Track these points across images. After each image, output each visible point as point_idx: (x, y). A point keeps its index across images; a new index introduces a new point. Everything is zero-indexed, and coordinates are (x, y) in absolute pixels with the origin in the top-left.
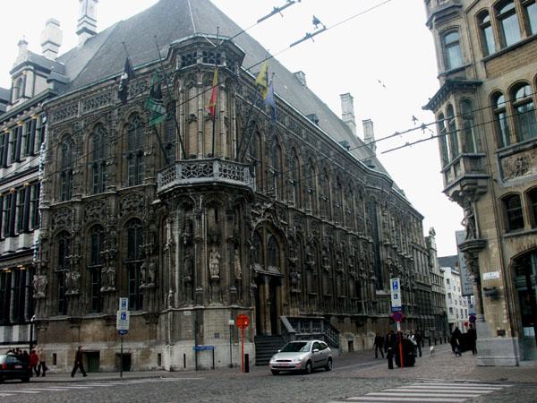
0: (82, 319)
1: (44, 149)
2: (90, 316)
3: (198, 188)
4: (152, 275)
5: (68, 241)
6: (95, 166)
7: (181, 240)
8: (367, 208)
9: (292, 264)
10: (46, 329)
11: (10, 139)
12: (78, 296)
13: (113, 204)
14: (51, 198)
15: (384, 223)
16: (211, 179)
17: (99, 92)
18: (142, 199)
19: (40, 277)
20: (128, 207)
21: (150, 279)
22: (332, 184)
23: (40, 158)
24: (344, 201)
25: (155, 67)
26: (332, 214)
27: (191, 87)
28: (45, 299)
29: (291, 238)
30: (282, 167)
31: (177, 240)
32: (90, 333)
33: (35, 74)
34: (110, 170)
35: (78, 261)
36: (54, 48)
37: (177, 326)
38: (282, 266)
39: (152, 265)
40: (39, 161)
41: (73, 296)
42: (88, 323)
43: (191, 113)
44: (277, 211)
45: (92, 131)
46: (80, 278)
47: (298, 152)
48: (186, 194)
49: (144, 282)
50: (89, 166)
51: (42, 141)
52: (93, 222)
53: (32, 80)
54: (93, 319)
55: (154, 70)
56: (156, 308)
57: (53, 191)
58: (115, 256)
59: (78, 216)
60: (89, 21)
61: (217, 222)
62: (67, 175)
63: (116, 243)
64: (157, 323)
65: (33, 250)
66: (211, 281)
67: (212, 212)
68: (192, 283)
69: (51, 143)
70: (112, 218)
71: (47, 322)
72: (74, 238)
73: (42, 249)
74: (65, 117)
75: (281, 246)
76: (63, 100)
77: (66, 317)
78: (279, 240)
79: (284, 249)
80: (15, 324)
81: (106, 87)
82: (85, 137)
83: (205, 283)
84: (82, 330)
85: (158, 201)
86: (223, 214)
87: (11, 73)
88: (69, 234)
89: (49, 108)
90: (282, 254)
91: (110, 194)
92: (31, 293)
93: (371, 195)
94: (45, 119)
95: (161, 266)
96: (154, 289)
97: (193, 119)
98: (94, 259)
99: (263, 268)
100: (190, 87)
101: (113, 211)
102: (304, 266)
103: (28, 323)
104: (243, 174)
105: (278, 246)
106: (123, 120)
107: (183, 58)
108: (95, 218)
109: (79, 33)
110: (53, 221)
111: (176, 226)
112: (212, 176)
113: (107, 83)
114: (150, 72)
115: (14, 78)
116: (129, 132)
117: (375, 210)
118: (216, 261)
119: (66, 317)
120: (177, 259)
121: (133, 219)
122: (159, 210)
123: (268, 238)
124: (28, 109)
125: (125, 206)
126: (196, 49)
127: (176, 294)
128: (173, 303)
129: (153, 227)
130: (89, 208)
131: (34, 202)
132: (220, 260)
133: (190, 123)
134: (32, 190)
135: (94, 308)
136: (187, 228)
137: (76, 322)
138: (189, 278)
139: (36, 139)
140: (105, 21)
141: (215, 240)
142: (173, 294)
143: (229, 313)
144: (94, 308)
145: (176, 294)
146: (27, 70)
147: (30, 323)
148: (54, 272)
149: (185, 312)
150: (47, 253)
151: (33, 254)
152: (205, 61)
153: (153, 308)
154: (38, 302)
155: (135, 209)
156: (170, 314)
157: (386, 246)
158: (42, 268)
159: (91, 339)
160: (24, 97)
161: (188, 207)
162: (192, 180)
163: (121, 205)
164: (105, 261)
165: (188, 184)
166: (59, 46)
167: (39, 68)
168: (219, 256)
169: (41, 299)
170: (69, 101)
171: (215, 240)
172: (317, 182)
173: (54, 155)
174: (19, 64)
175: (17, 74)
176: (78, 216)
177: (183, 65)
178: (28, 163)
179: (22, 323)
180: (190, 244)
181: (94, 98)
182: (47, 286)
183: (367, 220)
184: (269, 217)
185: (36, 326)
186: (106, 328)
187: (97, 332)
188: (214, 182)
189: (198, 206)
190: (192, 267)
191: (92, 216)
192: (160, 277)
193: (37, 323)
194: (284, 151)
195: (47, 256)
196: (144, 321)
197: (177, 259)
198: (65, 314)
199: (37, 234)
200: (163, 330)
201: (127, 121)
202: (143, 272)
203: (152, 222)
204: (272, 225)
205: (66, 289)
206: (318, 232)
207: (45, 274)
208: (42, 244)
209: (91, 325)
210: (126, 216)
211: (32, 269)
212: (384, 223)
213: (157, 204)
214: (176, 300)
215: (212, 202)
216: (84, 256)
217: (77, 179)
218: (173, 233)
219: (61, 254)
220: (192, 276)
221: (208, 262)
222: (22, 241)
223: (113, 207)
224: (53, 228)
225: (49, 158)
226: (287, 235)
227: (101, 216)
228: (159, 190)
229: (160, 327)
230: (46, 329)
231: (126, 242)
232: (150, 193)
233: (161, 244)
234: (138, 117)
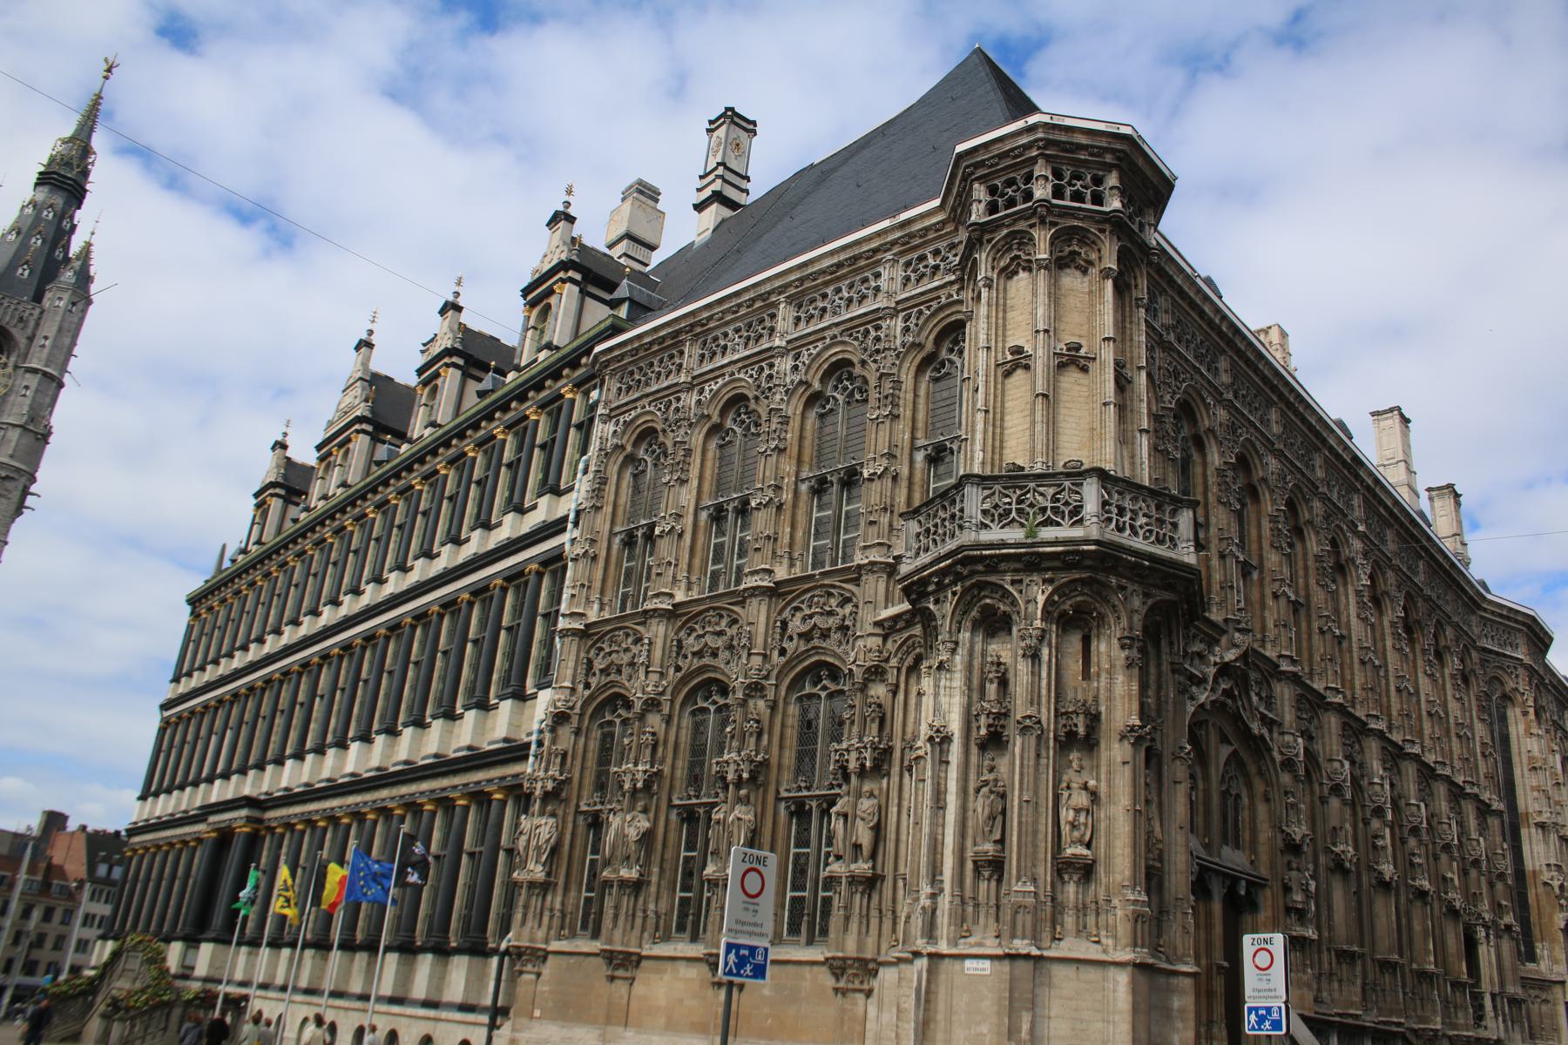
1: (585, 472)
3: (1031, 562)
4: (864, 836)
5: (625, 722)
6: (718, 515)
7: (969, 720)
8: (1481, 709)
9: (1293, 848)
11: (508, 455)
12: (637, 886)
13: (763, 619)
14: (588, 601)
15: (1531, 759)
16: (1078, 533)
18: (848, 609)
19: (537, 821)
20: (804, 628)
21: (857, 847)
22: (1393, 624)
23: (574, 495)
24: (1424, 683)
26: (1394, 713)
27: (1016, 273)
28: (545, 887)
29: (1288, 764)
30: (1261, 548)
31: (955, 726)
32: (662, 1002)
33: (584, 293)
34: (762, 521)
35: (648, 785)
36: (640, 252)
37: (941, 1007)
38: (1263, 850)
39: (866, 804)
40: (567, 505)
41: (623, 883)
42: (658, 972)
43: (1011, 343)
44: (1253, 675)
45: (716, 418)
46: (647, 838)
47: (1305, 515)
48: (993, 579)
49: (838, 858)
50: (704, 515)
51: (584, 451)
53: (574, 306)
56: (871, 941)
57: (597, 585)
58: (758, 774)
59: (657, 654)
60: (729, 176)
61: (1086, 674)
62: (639, 540)
63: (760, 735)
64: (869, 994)
65: (528, 745)
66: (1063, 867)
67: (1074, 643)
68: (996, 866)
70: (757, 661)
71: (544, 956)
72: (641, 717)
73: (554, 741)
74: (647, 384)
75: (1259, 787)
77: (596, 946)
78: (1252, 769)
79: (1267, 800)
80: (459, 951)
82: (697, 438)
83: (1045, 872)
84: (638, 988)
85: (906, 606)
86: (1108, 649)
87: (526, 292)
88: (628, 705)
89: (607, 364)
90: (1262, 809)
91: (755, 591)
92: (511, 868)
93: (1491, 672)
94: (594, 395)
95: (893, 810)
96: (871, 883)
97: (1019, 361)
98: (695, 780)
99: (1207, 846)
100: (1008, 273)
101: (760, 640)
102: (1322, 859)
103: (495, 951)
104: (1175, 526)
105: (1249, 785)
106: (808, 385)
107: (993, 191)
108: (707, 660)
109: (699, 207)
110: (590, 662)
111: (958, 680)
112: (1080, 521)
115: (532, 304)
116: (822, 416)
117: (1503, 719)
118: (1081, 799)
120: (952, 786)
121: (821, 664)
122: (900, 638)
123: (1222, 760)
124: (556, 375)
125: (796, 625)
126: (1034, 160)
127: (945, 902)
128: (930, 932)
129: (879, 691)
130: (693, 630)
131: (546, 616)
132: (1094, 795)
133: (1008, 374)
135: (681, 928)
136: (992, 689)
137: (623, 963)
138: (989, 847)
139: (569, 450)
140: (768, 167)
141: (1081, 730)
142: (933, 896)
143: (1123, 978)
144: (681, 928)
145: (945, 902)
146: (564, 281)
147: (495, 951)
148: (577, 812)
149: (968, 963)
150: (564, 756)
151: (526, 757)
152: (1058, 192)
153: (861, 945)
154: (524, 891)
155: (825, 635)
156: (922, 963)
157: (1542, 826)
158: (547, 797)
159: (662, 1021)
160: (549, 346)
161: (995, 624)
162: (1015, 534)
163: (784, 624)
164: (726, 788)
165: (1004, 545)
166: (652, 248)
167: (590, 272)
168: (1092, 783)
169: (532, 885)
170: (664, 338)
171: (1081, 730)
172: (1353, 610)
173: (610, 488)
174: (547, 267)
175: (538, 295)
176: (657, 654)
177: (992, 208)
178: (544, 510)
179: (477, 949)
180: (995, 741)
182: (555, 851)
183: (1483, 744)
184: (1228, 693)
185: (512, 964)
187: (682, 1000)
188: (1087, 542)
189: (1029, 618)
190: (999, 815)
191: (699, 654)
192: (891, 846)
193: (516, 954)
194: (1268, 507)
195: (563, 764)
197: (952, 786)
198: (596, 935)
199: (544, 703)
200: (889, 1016)
201: (817, 385)
202: (838, 825)
203: (876, 673)
204: (1237, 718)
205: (607, 863)
206: (1358, 758)
207: (553, 815)
208: (553, 730)
209: (666, 977)
210: (799, 658)
211: (520, 796)
212: (1531, 759)
213: (895, 618)
214: (943, 920)
215: (1078, 609)
216: (667, 770)
217: (665, 548)
218: (941, 702)
219: (604, 758)
220: (1001, 841)
221: (1057, 798)
222: (502, 723)
223: (761, 629)
224: (587, 686)
225: (597, 492)
226: (1278, 757)
227: (724, 655)
228: (904, 569)
229: (880, 1008)
230: (539, 975)
231: (792, 734)
232: (874, 586)
233: (898, 745)
234: (851, 378)
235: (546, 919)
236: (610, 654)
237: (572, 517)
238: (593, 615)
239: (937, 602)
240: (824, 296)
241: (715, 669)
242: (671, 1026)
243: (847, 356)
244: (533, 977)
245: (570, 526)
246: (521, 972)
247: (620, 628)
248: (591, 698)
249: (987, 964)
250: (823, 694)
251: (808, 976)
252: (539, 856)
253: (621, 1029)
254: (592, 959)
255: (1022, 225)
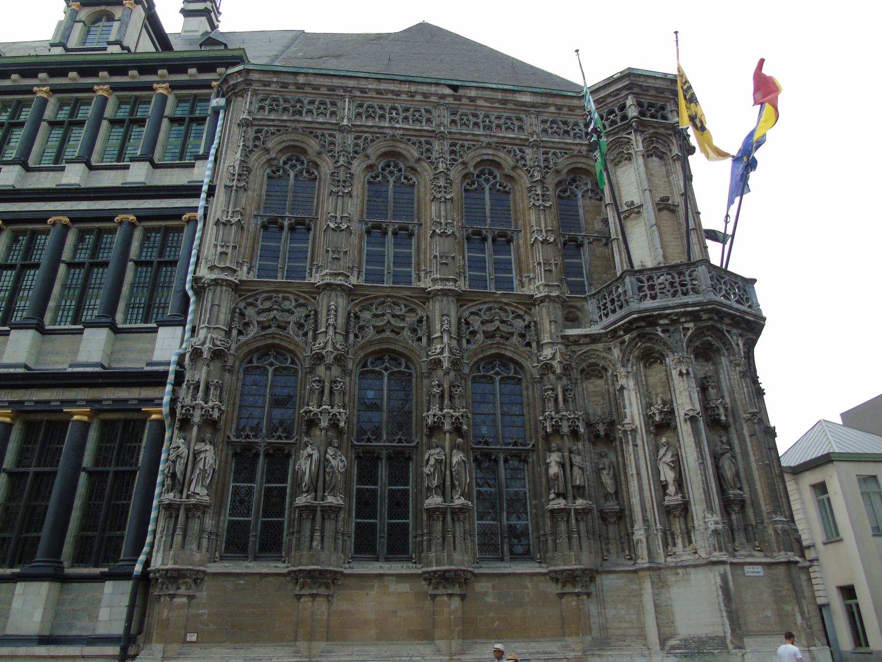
0: (342, 573)
2: (359, 568)
10: (191, 597)
17: (404, 97)
20: (490, 328)
25: (551, 100)
27: (651, 155)
48: (719, 325)
49: (558, 495)
52: (379, 342)
54: (380, 576)
55: (546, 105)
59: (341, 320)
69: (247, 152)
71: (198, 578)
76: (301, 79)
81: (426, 95)
84: (340, 604)
89: (248, 82)
113: (433, 89)
114: (533, 105)
119: (280, 567)
134: (138, 235)
149: (747, 568)
170: (317, 88)
181: (387, 105)
186: (428, 603)
191: (379, 330)
196: (553, 589)
209: (373, 593)
235: (205, 542)
236: (270, 310)
237: (205, 188)
238: (243, 274)
239: (663, 331)
240: (475, 116)
241: (396, 342)
242: (384, 635)
243: (496, 159)
244: (185, 600)
245: (203, 195)
246: (173, 596)
247: (278, 292)
248: (246, 343)
249: (759, 568)
250: (498, 378)
251: (529, 585)
252: (204, 479)
253: (323, 645)
254: (271, 578)
255: (662, 131)
